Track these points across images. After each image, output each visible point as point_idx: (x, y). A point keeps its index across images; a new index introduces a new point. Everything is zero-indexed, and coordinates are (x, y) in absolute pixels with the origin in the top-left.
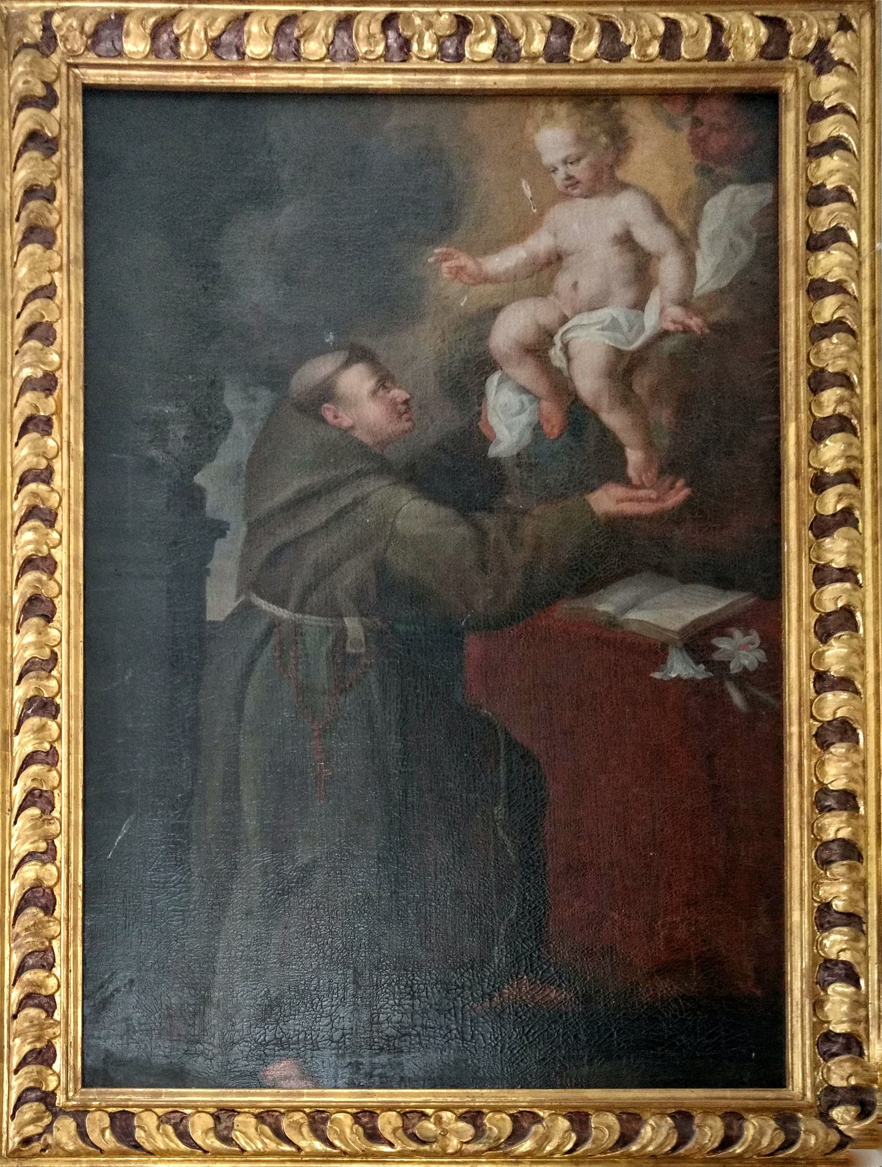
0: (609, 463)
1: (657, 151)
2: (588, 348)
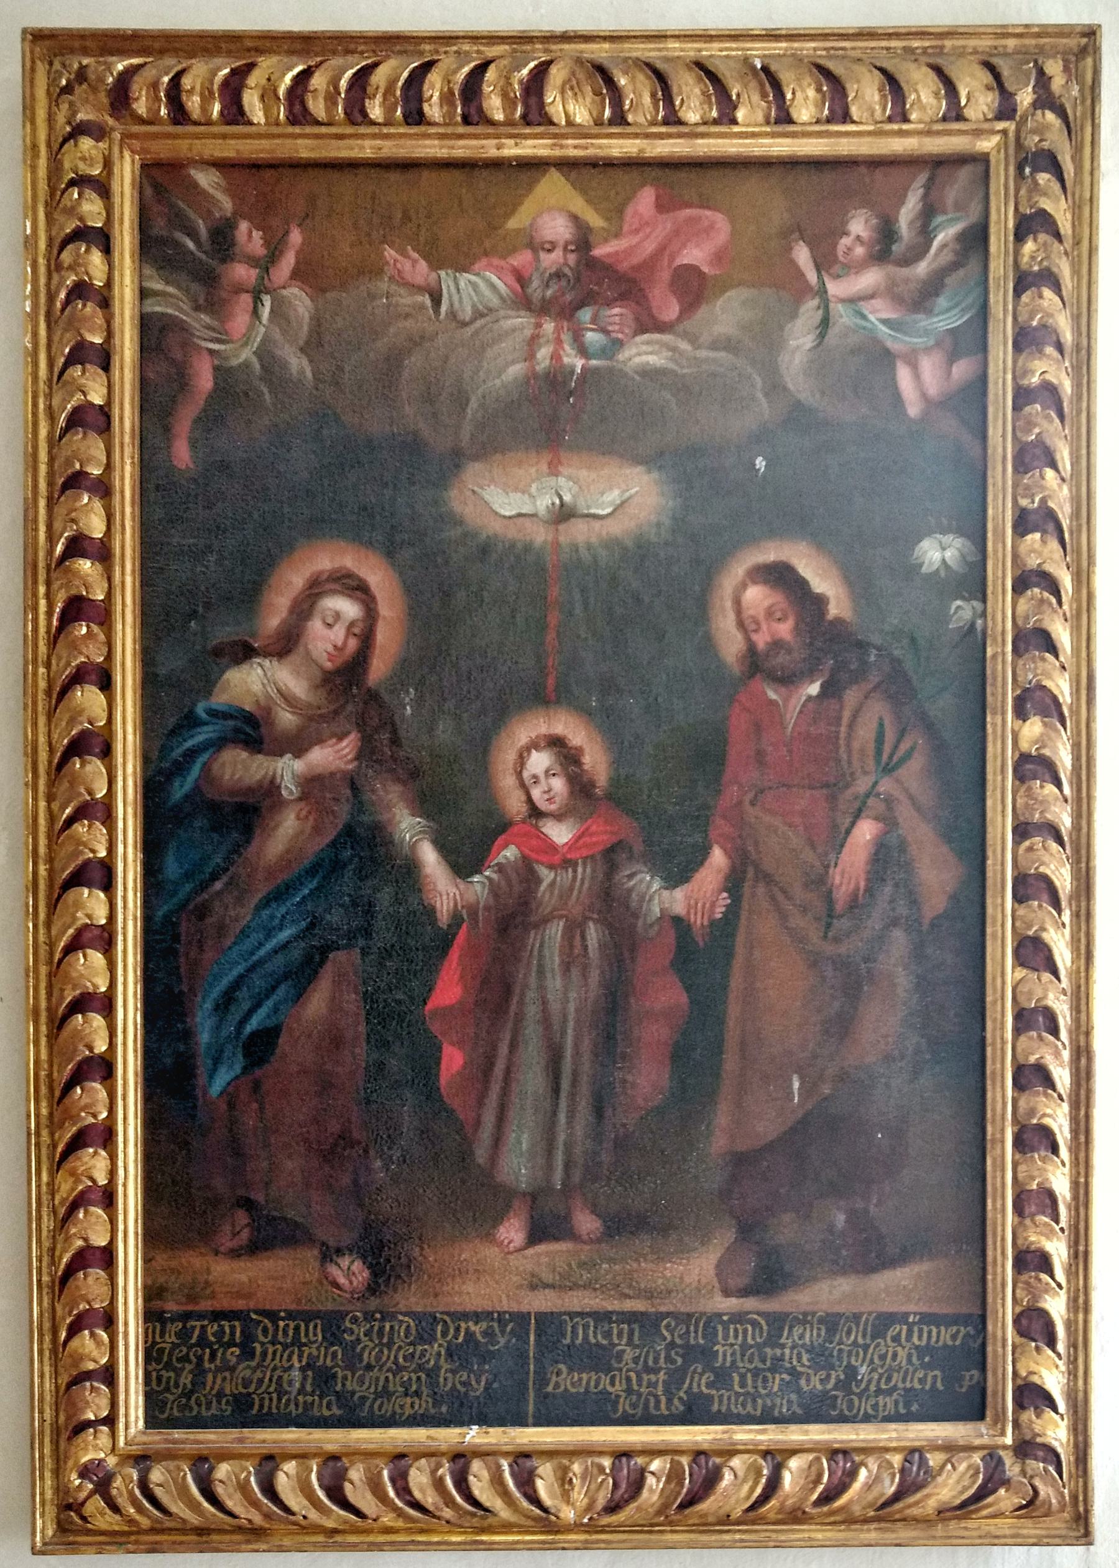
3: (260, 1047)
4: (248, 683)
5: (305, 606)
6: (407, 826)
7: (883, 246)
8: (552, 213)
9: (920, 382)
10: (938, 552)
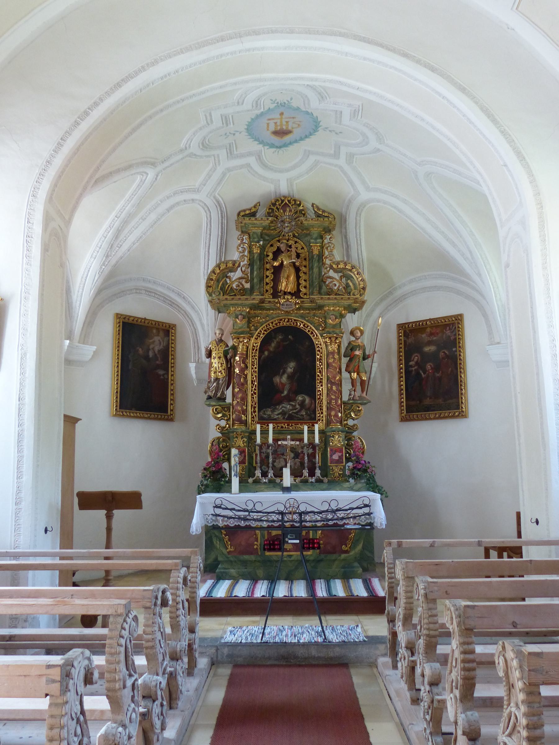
0: (158, 360)
1: (161, 333)
2: (157, 349)
4: (411, 363)
6: (421, 371)
7: (450, 329)
8: (428, 330)
9: (452, 338)
10: (454, 349)
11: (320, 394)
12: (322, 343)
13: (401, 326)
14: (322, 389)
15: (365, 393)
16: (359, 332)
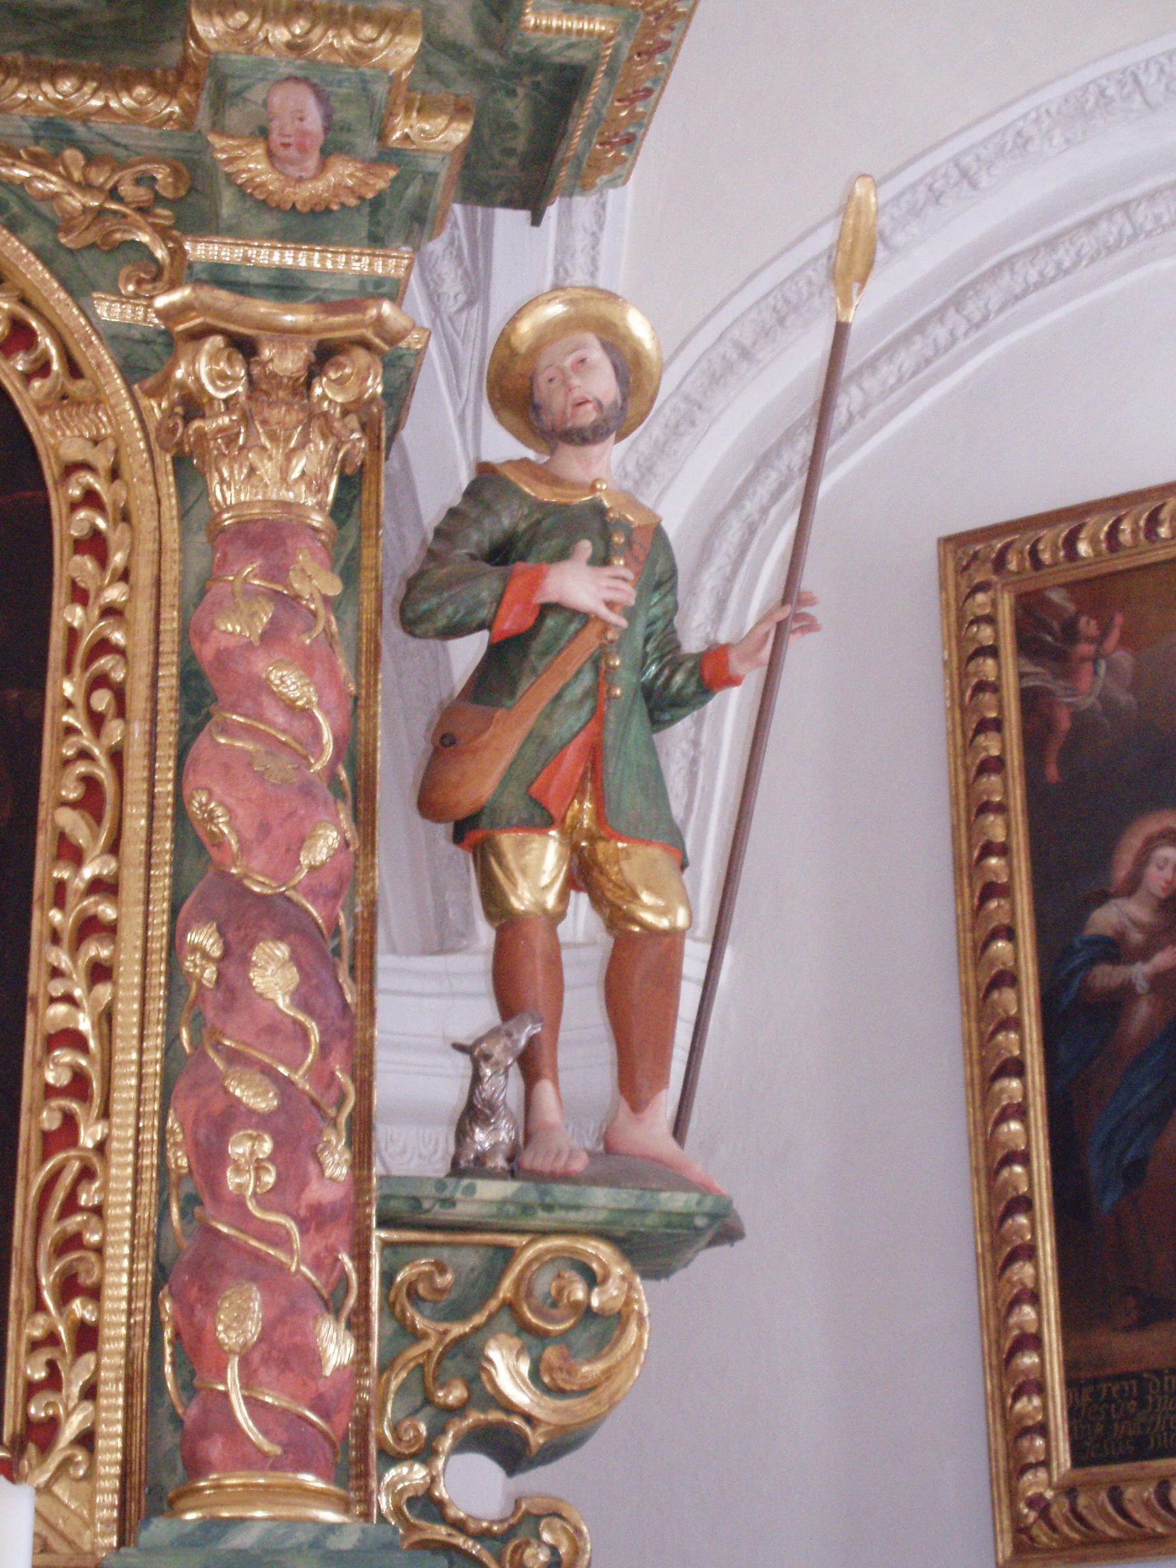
3: (1135, 1172)
4: (1106, 918)
5: (1143, 859)
11: (79, 1086)
12: (136, 462)
13: (973, 556)
14: (106, 1018)
15: (667, 1101)
16: (596, 354)
